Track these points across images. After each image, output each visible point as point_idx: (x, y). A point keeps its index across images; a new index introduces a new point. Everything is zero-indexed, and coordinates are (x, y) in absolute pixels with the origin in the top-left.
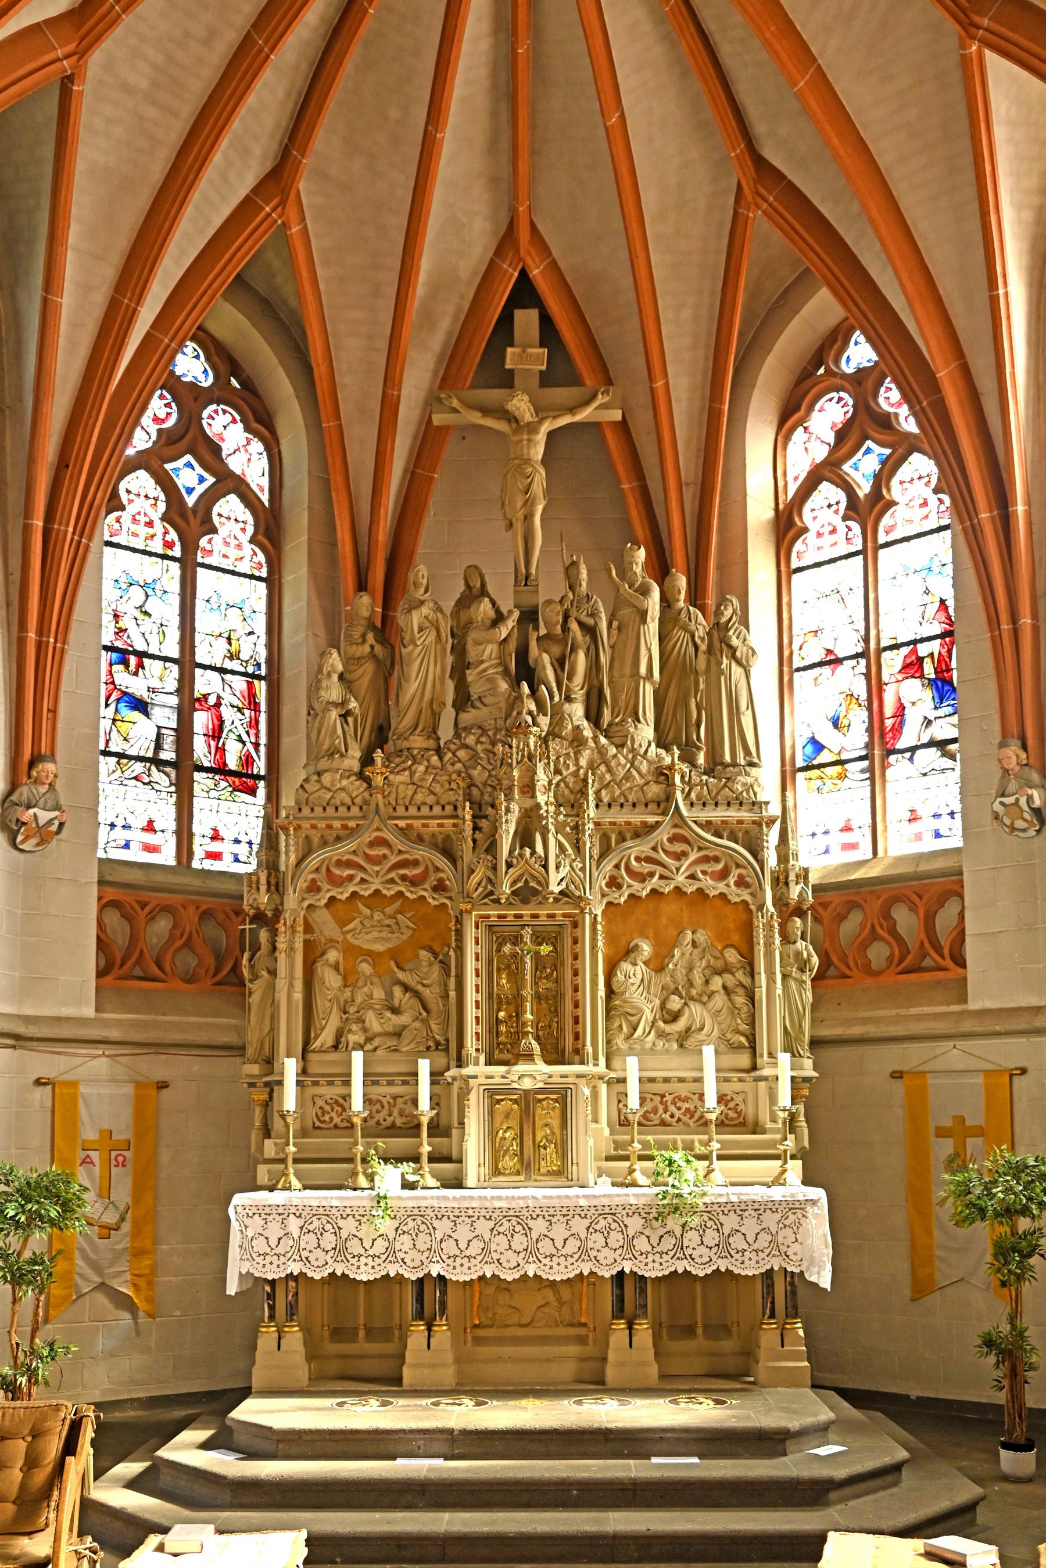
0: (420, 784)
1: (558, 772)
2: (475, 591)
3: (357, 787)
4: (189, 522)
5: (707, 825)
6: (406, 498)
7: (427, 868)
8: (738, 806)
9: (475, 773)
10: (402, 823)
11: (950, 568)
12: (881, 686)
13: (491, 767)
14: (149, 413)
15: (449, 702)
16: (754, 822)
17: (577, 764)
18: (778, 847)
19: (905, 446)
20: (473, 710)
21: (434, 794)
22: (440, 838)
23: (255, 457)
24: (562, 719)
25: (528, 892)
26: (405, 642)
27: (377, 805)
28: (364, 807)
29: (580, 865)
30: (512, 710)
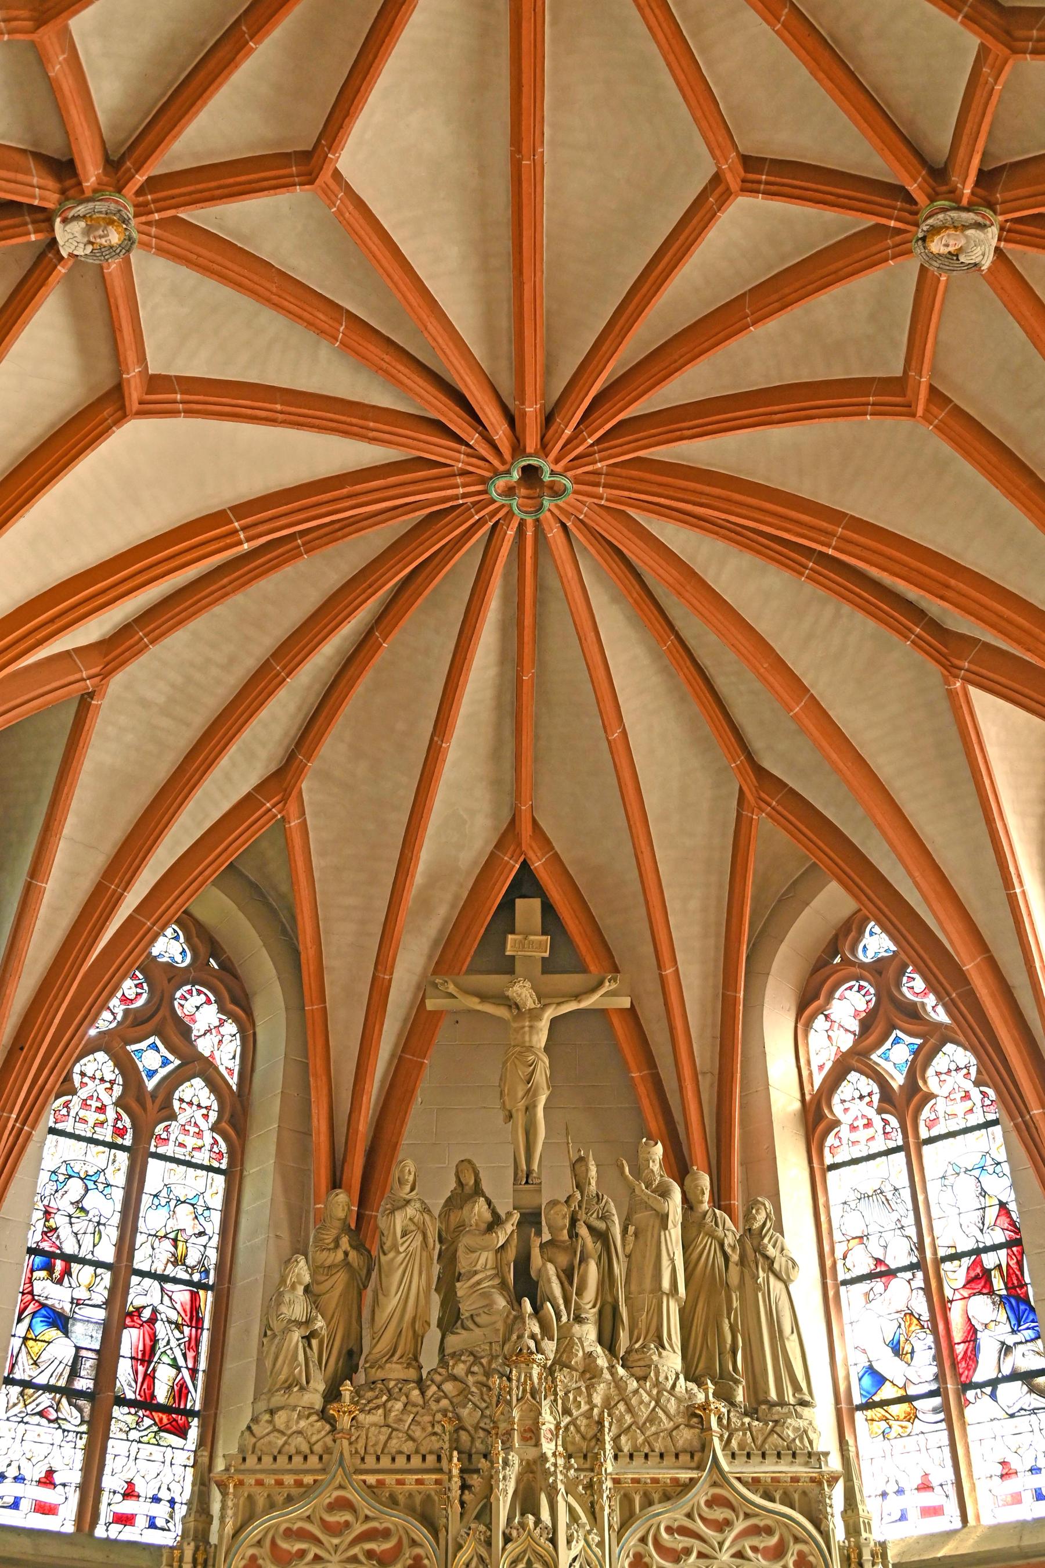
0: (395, 1426)
1: (566, 1412)
2: (468, 1190)
3: (317, 1429)
4: (145, 1110)
5: (753, 1484)
6: (392, 1086)
7: (400, 1542)
8: (790, 1458)
9: (465, 1412)
10: (371, 1479)
11: (1006, 1168)
12: (945, 1304)
13: (484, 1405)
14: (119, 994)
15: (434, 1322)
16: (812, 1480)
17: (590, 1401)
18: (844, 1513)
19: (937, 1035)
20: (463, 1332)
21: (411, 1438)
22: (418, 1499)
23: (227, 1039)
24: (571, 1345)
26: (385, 1248)
27: (342, 1454)
28: (325, 1457)
29: (597, 1539)
30: (511, 1332)
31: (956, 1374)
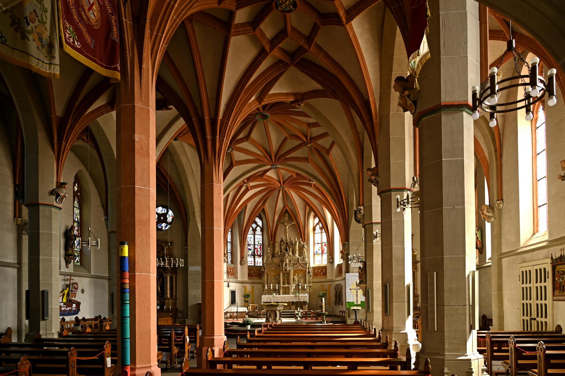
4: (254, 230)
25: (286, 270)
31: (323, 253)
